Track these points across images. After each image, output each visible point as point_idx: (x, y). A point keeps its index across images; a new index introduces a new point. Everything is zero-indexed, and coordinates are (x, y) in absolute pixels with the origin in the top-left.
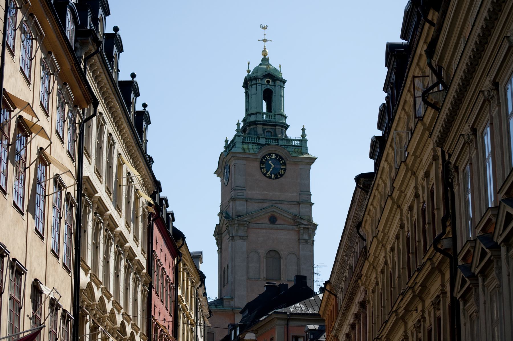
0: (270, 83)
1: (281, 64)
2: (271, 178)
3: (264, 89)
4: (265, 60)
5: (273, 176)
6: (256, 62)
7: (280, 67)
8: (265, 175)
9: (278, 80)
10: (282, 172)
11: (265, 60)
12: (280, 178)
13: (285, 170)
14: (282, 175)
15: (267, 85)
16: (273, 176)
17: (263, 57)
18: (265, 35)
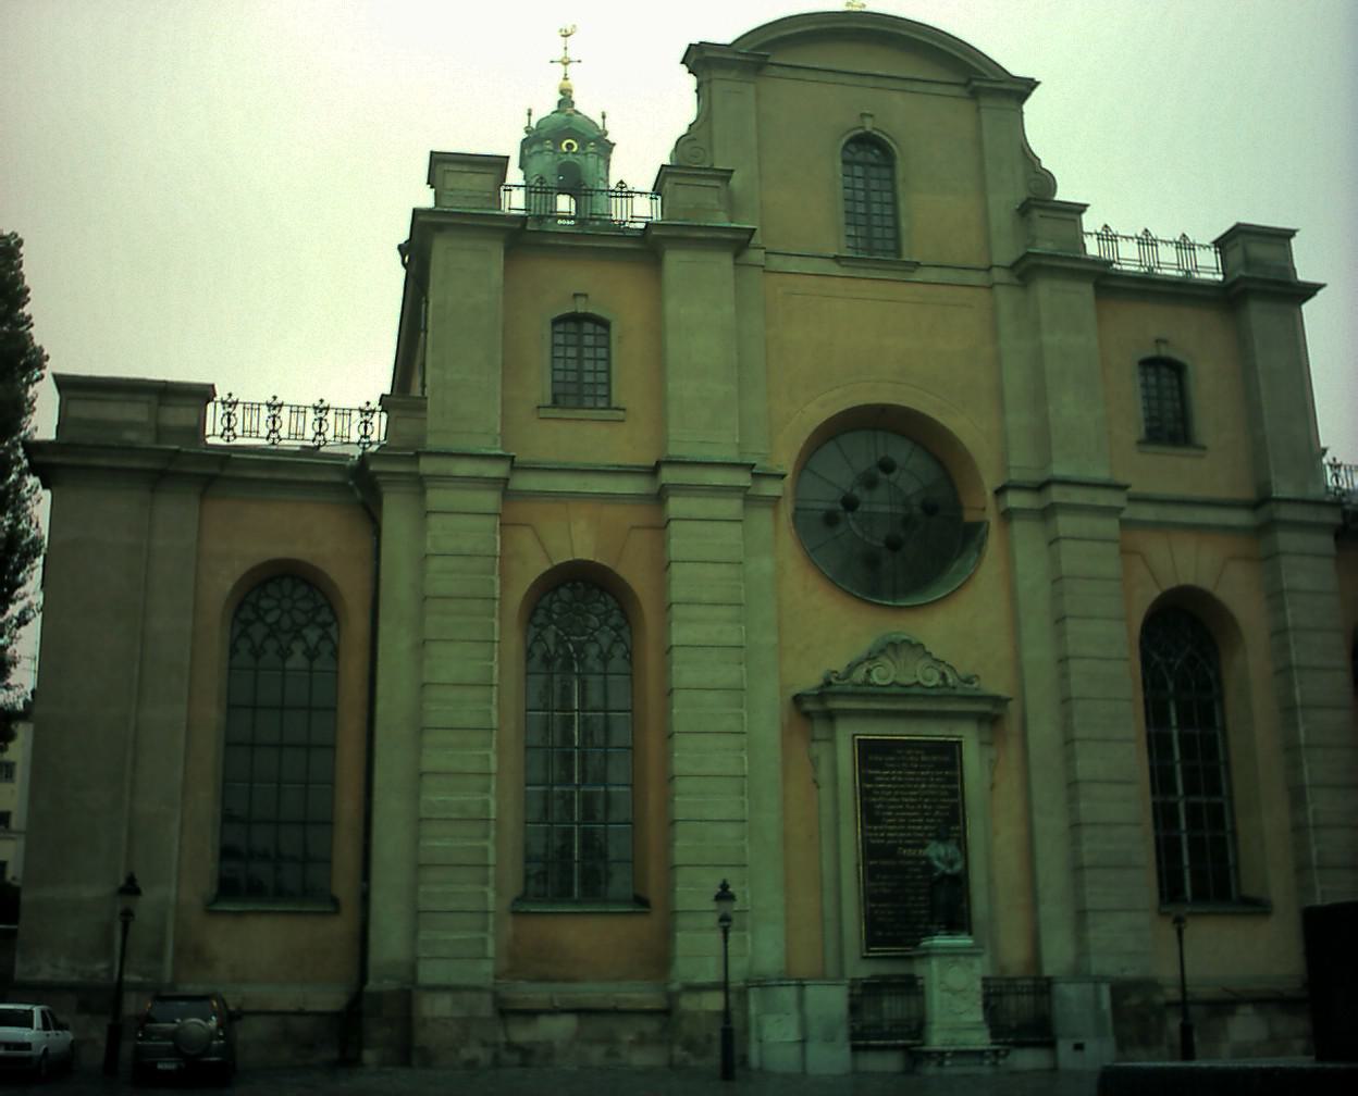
0: (575, 150)
1: (605, 111)
3: (560, 162)
4: (566, 100)
6: (546, 106)
7: (604, 117)
11: (566, 100)
17: (561, 97)
18: (566, 48)
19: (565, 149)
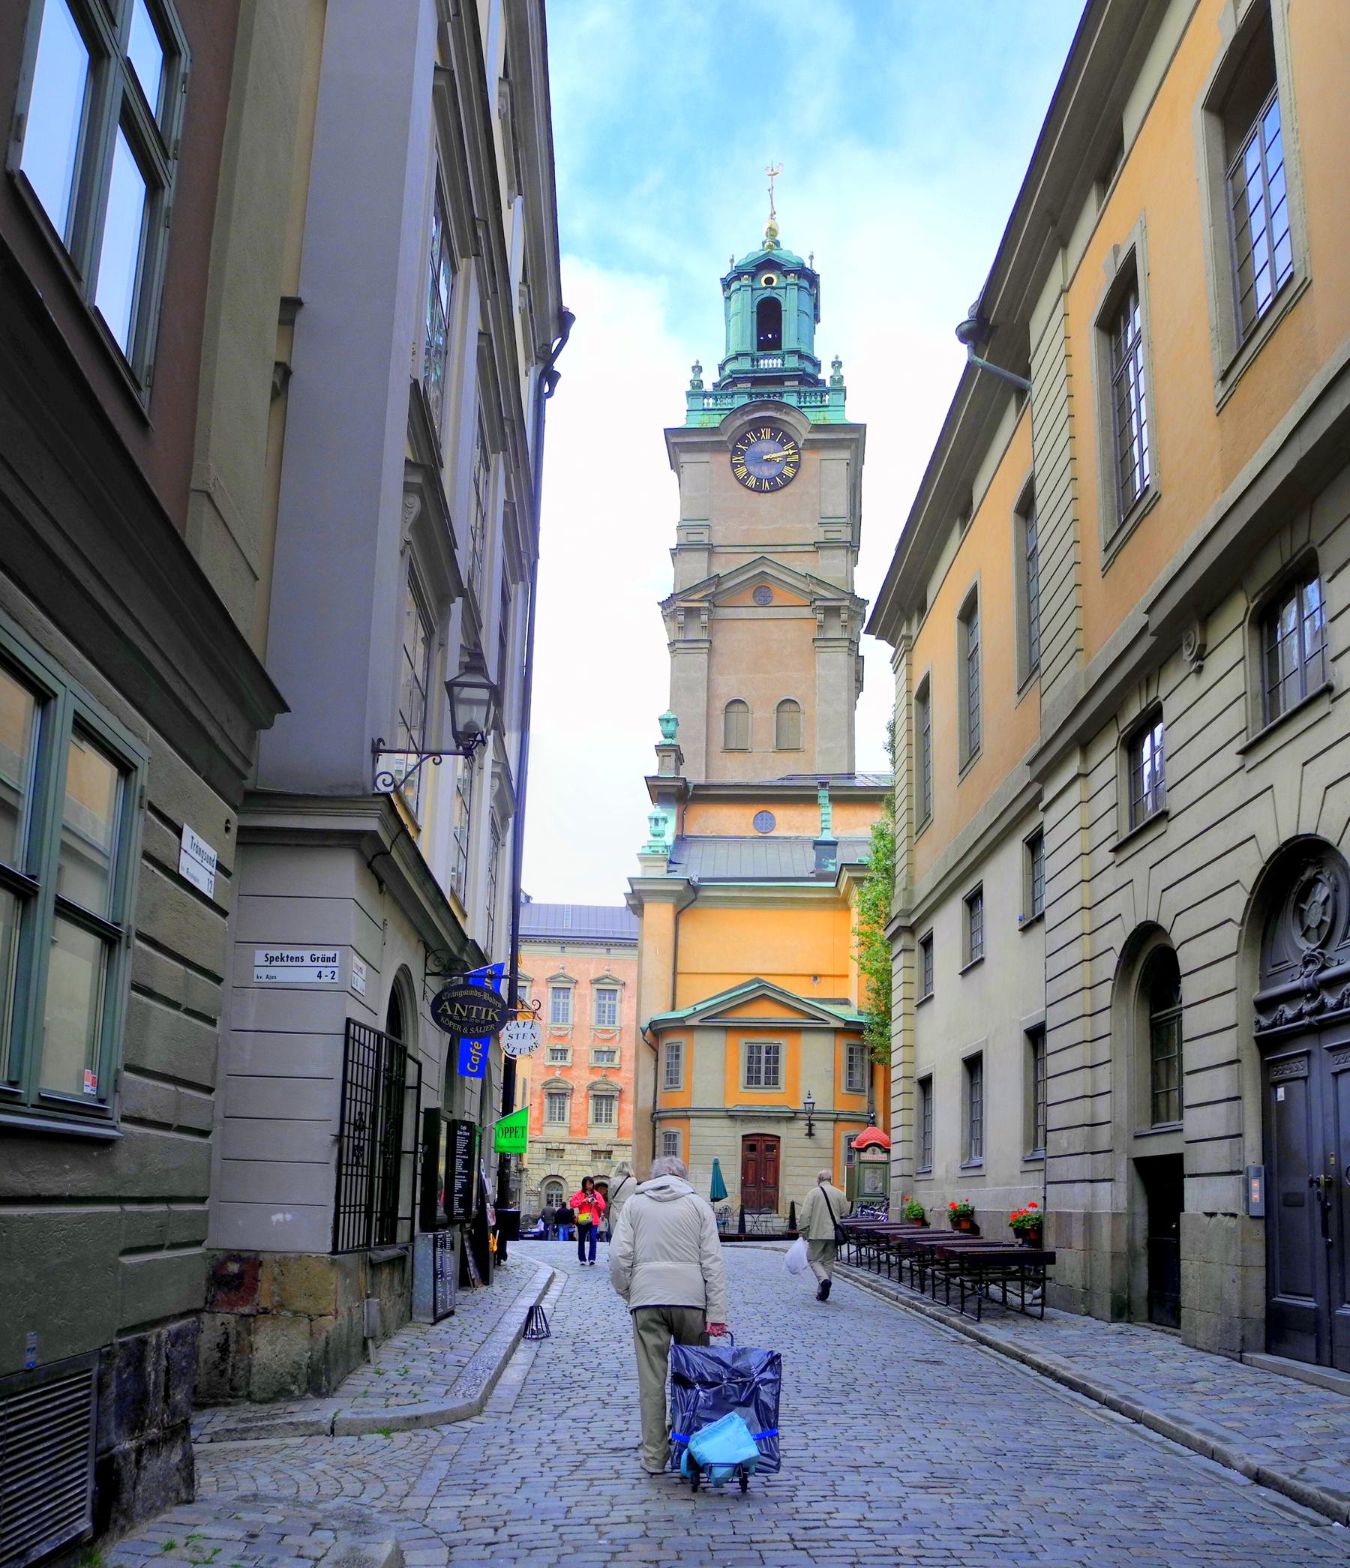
2: (758, 489)
5: (766, 485)
7: (812, 257)
8: (742, 482)
9: (792, 272)
10: (788, 471)
12: (783, 487)
13: (797, 466)
14: (788, 481)
15: (766, 288)
16: (766, 485)
19: (764, 285)
